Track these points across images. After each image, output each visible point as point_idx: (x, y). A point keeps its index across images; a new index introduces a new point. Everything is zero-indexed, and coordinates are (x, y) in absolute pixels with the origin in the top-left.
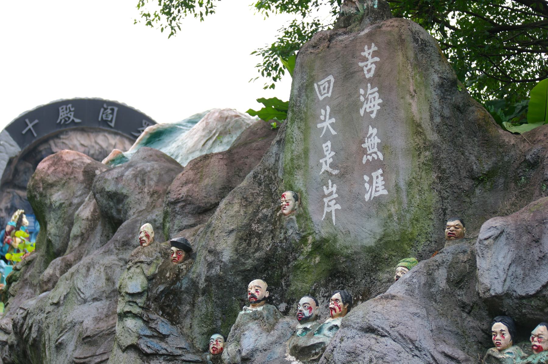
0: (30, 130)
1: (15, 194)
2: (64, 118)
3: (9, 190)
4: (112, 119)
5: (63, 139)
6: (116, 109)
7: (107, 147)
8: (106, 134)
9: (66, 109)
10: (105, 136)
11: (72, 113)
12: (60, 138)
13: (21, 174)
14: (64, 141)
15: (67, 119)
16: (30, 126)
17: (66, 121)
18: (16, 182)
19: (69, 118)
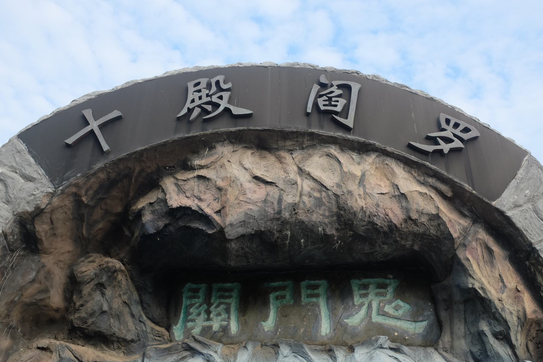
0: (92, 132)
1: (67, 354)
2: (199, 106)
3: (44, 342)
4: (346, 108)
5: (201, 167)
6: (356, 88)
7: (338, 186)
8: (334, 150)
9: (209, 86)
10: (329, 155)
11: (226, 95)
12: (192, 169)
13: (86, 290)
14: (203, 172)
15: (209, 108)
16: (94, 125)
17: (205, 111)
18: (74, 317)
19: (216, 106)
